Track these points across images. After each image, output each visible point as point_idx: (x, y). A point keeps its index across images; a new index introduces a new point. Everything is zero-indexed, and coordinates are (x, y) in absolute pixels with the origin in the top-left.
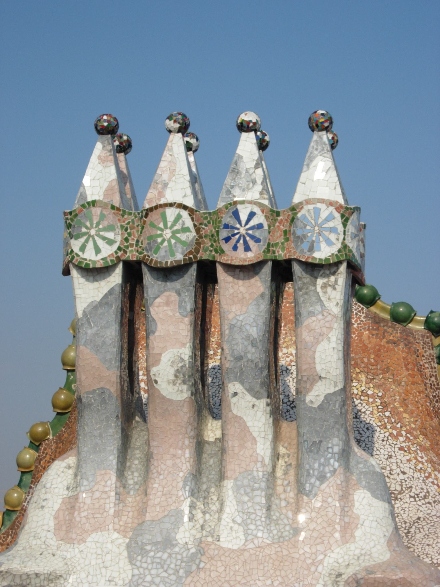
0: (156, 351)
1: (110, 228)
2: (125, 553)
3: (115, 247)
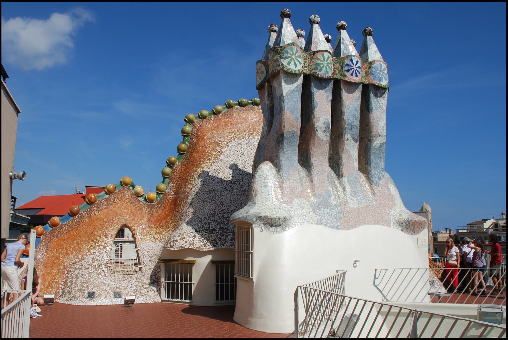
0: (318, 116)
1: (300, 57)
2: (311, 209)
3: (302, 65)
